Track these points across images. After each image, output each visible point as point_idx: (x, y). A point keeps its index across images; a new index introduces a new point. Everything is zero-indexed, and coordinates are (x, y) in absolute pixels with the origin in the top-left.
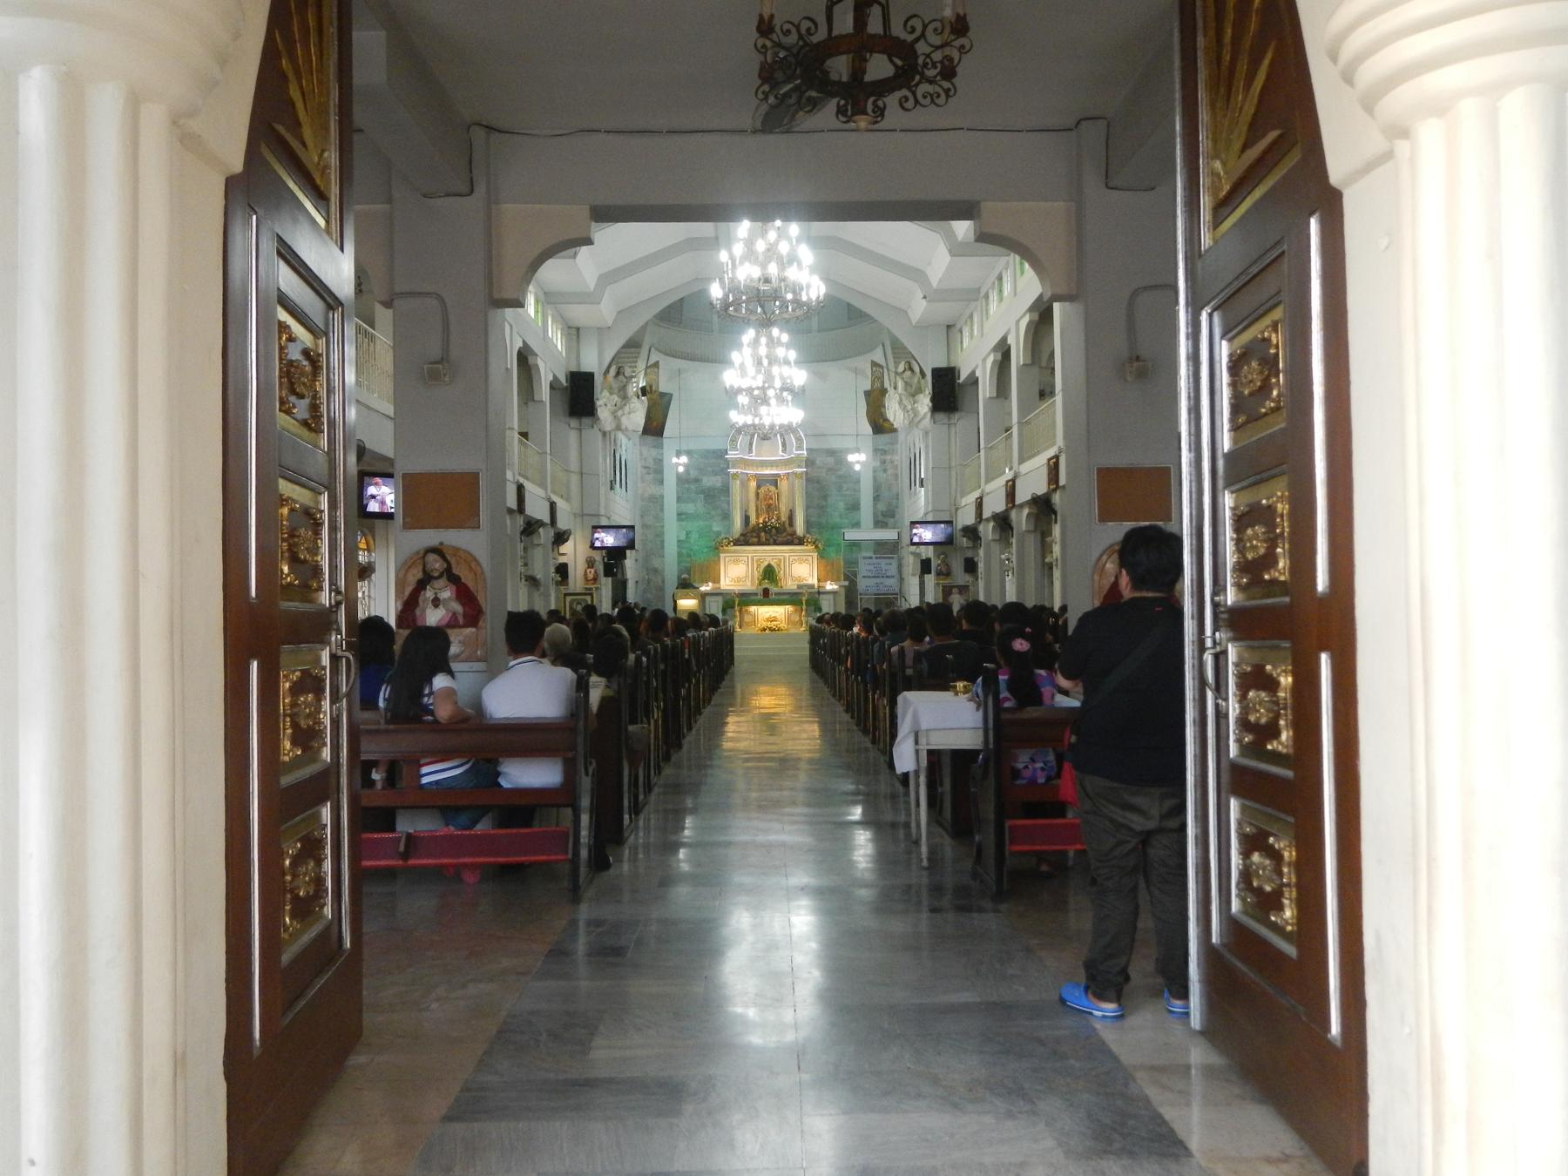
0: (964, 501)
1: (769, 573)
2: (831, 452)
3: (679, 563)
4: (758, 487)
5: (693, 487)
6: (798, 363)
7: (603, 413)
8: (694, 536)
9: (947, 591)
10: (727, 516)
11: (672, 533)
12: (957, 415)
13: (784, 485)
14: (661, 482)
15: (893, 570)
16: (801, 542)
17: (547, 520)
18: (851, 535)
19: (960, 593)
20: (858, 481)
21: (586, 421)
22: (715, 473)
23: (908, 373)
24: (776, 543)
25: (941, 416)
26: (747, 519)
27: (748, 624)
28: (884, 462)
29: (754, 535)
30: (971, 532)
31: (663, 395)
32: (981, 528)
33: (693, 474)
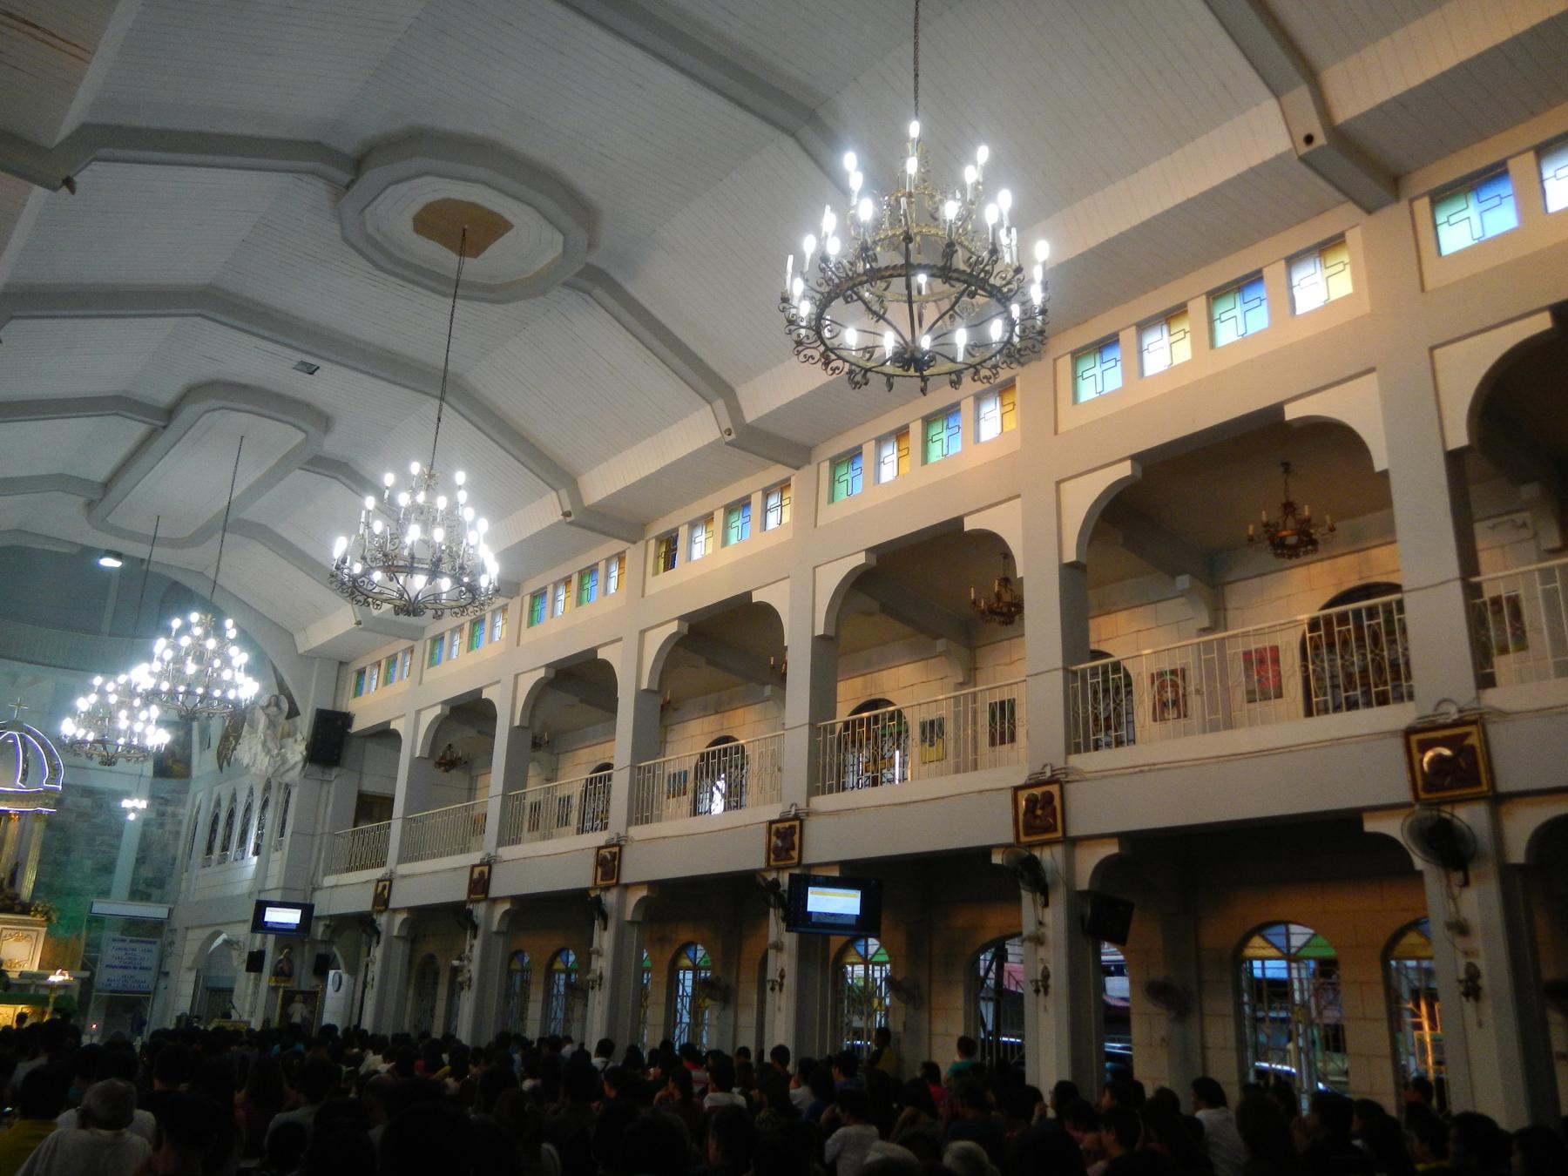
0: (329, 881)
2: (89, 792)
6: (250, 670)
9: (289, 998)
12: (335, 771)
13: (13, 827)
15: (151, 960)
16: (25, 909)
18: (100, 907)
19: (305, 1002)
20: (119, 835)
23: (273, 710)
25: (315, 769)
28: (162, 814)
30: (362, 925)
32: (382, 920)
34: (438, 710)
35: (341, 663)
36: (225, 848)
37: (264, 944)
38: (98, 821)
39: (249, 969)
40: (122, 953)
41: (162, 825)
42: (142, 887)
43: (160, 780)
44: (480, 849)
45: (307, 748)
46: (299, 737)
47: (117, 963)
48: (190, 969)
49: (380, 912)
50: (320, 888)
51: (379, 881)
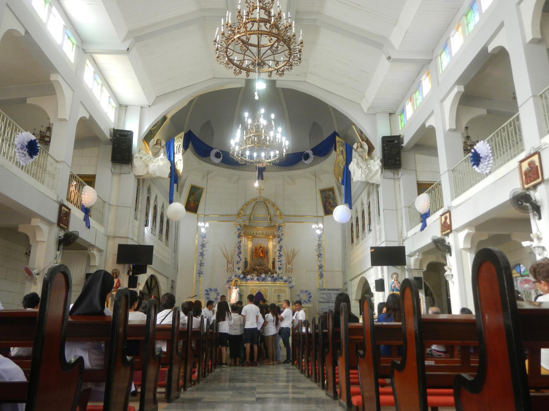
0: (411, 233)
7: (137, 162)
12: (401, 172)
17: (54, 218)
21: (125, 168)
23: (360, 150)
25: (389, 174)
32: (450, 240)
34: (455, 90)
35: (390, 114)
36: (358, 237)
37: (383, 276)
39: (377, 290)
40: (325, 296)
44: (523, 150)
45: (381, 161)
46: (376, 158)
47: (323, 300)
49: (447, 235)
50: (407, 238)
51: (441, 216)
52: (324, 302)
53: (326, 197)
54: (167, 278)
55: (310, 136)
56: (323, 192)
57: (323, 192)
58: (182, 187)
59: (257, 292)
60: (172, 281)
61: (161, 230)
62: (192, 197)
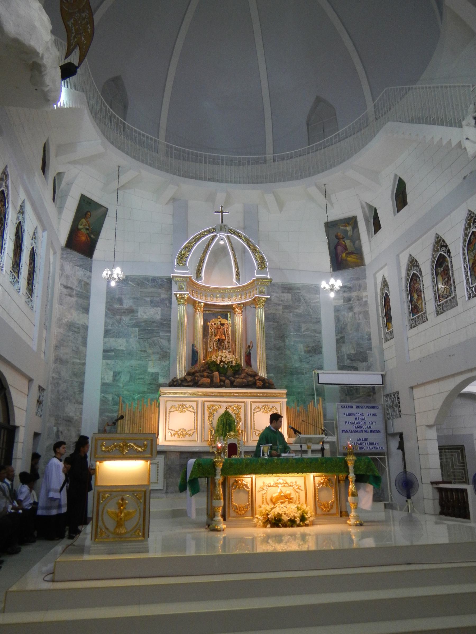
1: (227, 424)
2: (288, 288)
3: (102, 412)
4: (205, 321)
5: (126, 319)
8: (124, 378)
10: (165, 355)
11: (96, 372)
14: (86, 310)
16: (266, 384)
20: (318, 322)
22: (154, 304)
24: (232, 385)
26: (194, 354)
27: (239, 512)
29: (205, 374)
31: (98, 206)
33: (127, 303)
38: (299, 311)
40: (352, 419)
41: (351, 309)
42: (347, 362)
43: (337, 272)
47: (349, 427)
48: (430, 426)
52: (350, 431)
53: (337, 237)
54: (30, 380)
55: (308, 125)
56: (330, 226)
57: (330, 226)
58: (66, 195)
59: (222, 411)
60: (40, 387)
61: (16, 265)
62: (83, 220)
